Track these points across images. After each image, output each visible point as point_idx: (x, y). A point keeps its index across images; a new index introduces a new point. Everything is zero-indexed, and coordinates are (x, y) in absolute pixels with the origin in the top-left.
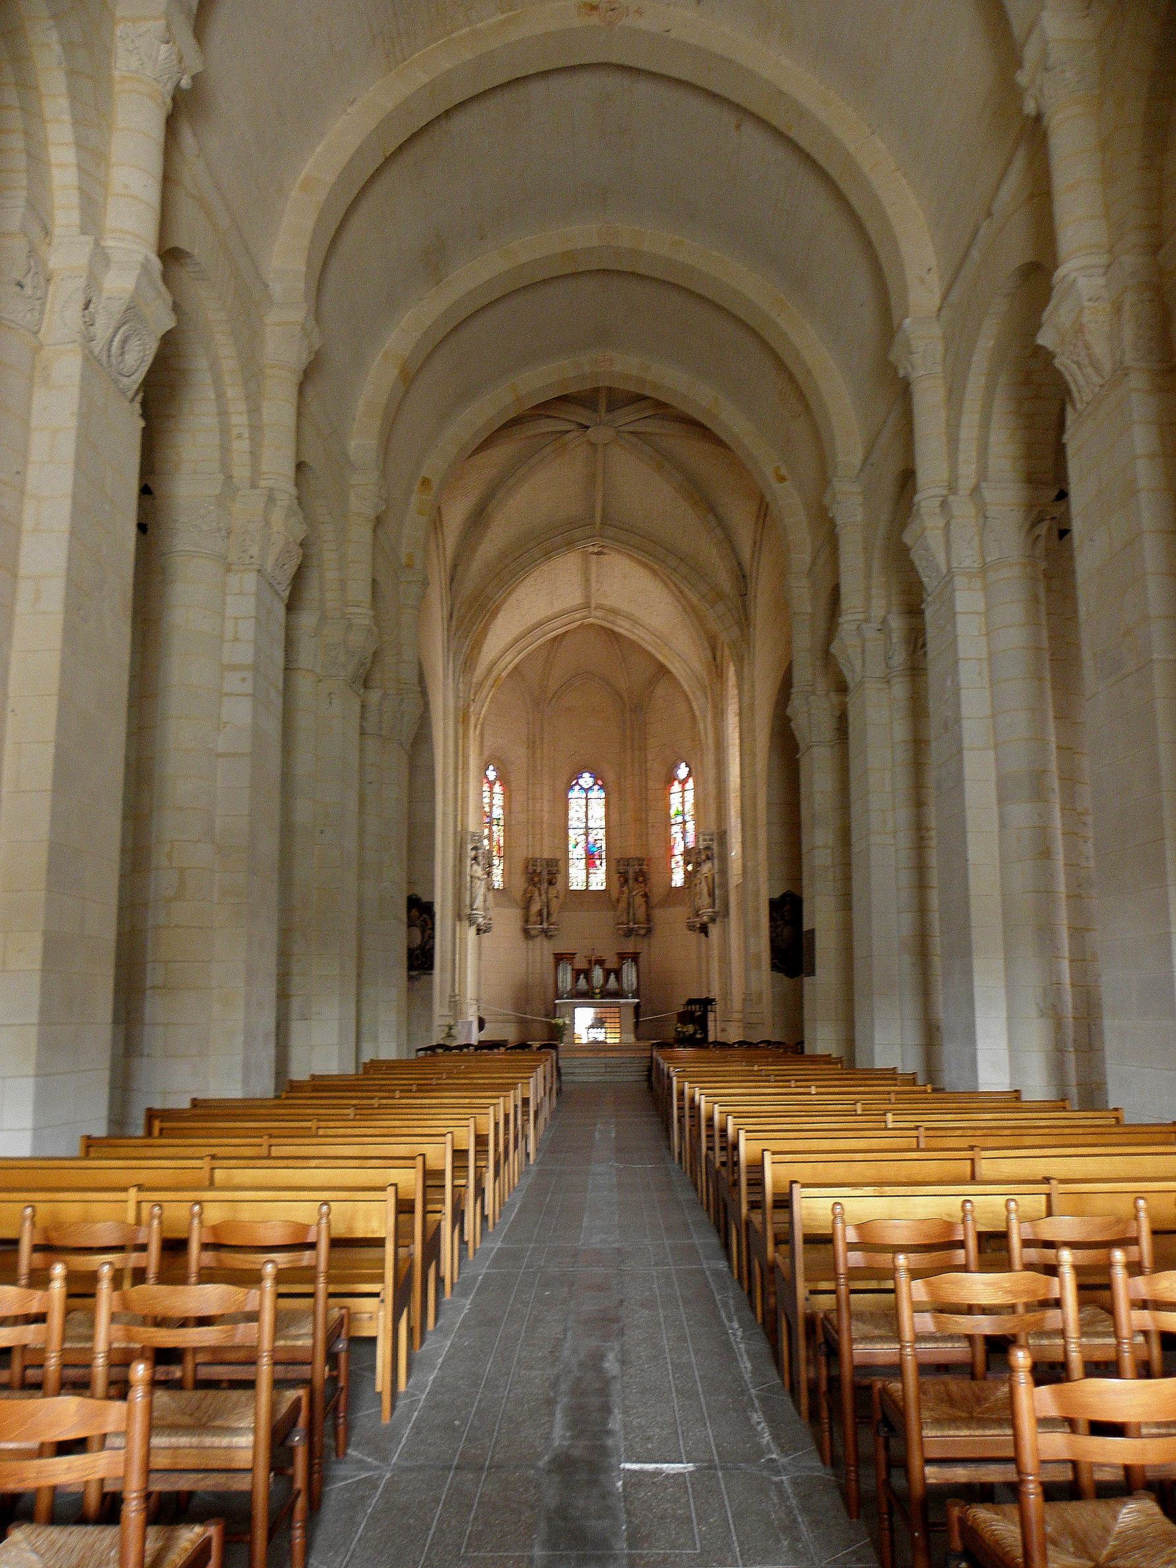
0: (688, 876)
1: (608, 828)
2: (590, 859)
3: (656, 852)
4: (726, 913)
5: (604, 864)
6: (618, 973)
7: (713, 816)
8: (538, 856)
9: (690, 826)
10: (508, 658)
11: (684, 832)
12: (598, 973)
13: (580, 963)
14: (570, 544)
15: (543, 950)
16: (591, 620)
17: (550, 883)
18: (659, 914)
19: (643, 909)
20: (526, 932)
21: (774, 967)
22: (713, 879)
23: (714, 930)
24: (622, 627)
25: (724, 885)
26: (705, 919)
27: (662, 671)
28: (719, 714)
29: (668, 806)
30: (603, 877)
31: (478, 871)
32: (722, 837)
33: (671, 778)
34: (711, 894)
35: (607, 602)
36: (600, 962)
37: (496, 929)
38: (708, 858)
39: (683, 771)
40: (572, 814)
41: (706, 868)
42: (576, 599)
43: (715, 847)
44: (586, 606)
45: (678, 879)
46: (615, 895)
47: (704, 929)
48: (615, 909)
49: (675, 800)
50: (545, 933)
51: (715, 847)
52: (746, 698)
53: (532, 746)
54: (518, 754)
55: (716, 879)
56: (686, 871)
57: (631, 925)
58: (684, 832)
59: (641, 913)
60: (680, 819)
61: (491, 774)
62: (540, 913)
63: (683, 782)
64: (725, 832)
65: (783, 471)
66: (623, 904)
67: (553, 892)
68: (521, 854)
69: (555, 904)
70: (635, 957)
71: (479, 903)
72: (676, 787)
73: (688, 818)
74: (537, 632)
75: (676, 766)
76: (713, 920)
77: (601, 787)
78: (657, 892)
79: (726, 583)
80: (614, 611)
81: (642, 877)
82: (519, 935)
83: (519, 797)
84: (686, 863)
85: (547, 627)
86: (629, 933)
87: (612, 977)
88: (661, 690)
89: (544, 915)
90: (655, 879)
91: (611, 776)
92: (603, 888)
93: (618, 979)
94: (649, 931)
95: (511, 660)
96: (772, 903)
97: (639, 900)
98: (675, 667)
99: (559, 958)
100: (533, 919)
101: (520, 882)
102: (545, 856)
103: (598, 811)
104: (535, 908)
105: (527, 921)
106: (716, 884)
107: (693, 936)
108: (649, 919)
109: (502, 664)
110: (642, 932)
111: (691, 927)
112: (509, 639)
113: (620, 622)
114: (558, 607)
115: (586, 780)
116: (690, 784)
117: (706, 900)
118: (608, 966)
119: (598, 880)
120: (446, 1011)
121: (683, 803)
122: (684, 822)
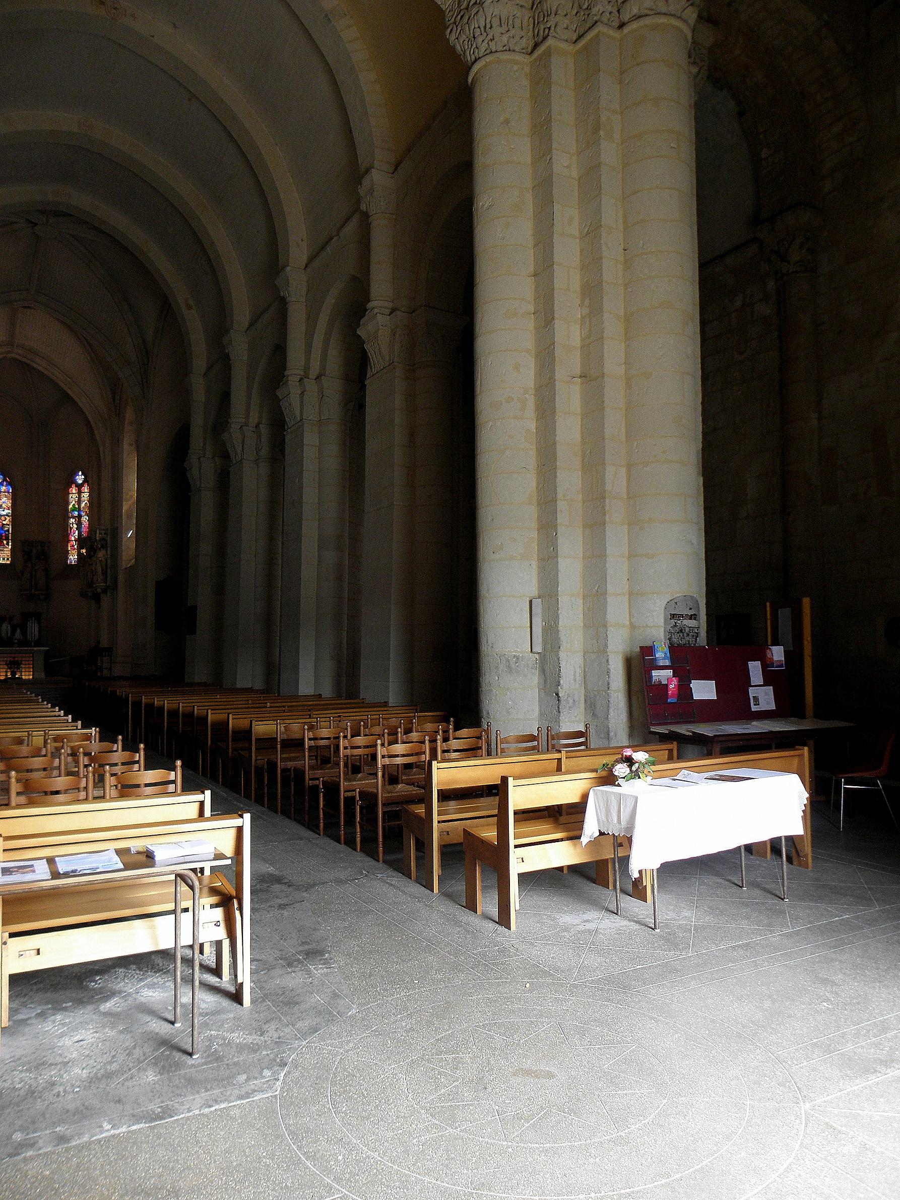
5: (10, 544)
9: (85, 519)
11: (79, 524)
16: (13, 355)
22: (107, 562)
23: (106, 600)
24: (40, 364)
25: (115, 566)
26: (99, 590)
27: (66, 398)
28: (117, 442)
29: (68, 503)
30: (9, 553)
33: (71, 482)
34: (104, 573)
38: (103, 547)
39: (80, 479)
41: (101, 554)
43: (109, 539)
45: (73, 558)
47: (97, 598)
51: (109, 539)
55: (109, 561)
56: (79, 554)
57: (33, 592)
58: (79, 524)
60: (76, 513)
63: (79, 487)
64: (117, 529)
65: (191, 302)
70: (38, 616)
72: (74, 490)
73: (83, 514)
76: (105, 591)
77: (9, 484)
84: (80, 547)
87: (18, 630)
92: (8, 562)
93: (24, 632)
96: (158, 584)
106: (108, 566)
110: (42, 597)
111: (84, 595)
117: (100, 577)
121: (79, 502)
122: (80, 516)
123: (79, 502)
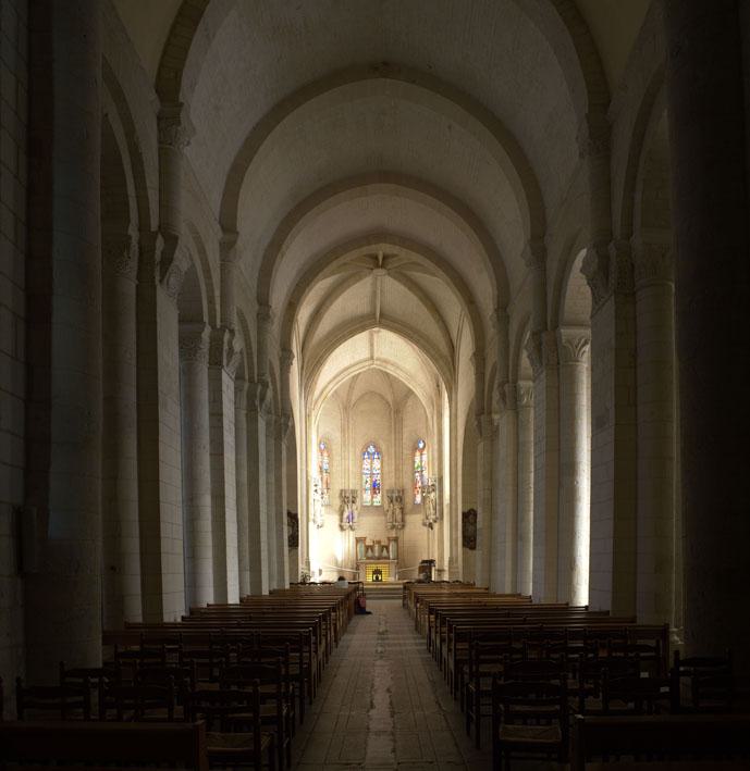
0: (424, 499)
1: (382, 474)
2: (375, 488)
3: (408, 486)
4: (442, 518)
6: (387, 548)
7: (436, 469)
8: (347, 488)
10: (331, 386)
12: (376, 548)
13: (369, 543)
14: (363, 329)
15: (351, 536)
17: (353, 502)
18: (409, 518)
19: (400, 516)
20: (342, 528)
21: (464, 545)
23: (436, 526)
24: (390, 370)
25: (441, 504)
27: (410, 392)
29: (414, 462)
31: (318, 497)
32: (441, 480)
33: (415, 448)
34: (435, 509)
35: (384, 356)
36: (379, 542)
37: (325, 524)
39: (421, 445)
40: (364, 466)
42: (366, 355)
44: (372, 358)
45: (418, 499)
46: (386, 507)
47: (431, 526)
48: (386, 515)
49: (417, 459)
50: (351, 527)
52: (453, 411)
53: (343, 431)
54: (337, 436)
58: (422, 476)
59: (399, 517)
61: (322, 446)
62: (348, 517)
66: (390, 513)
67: (354, 507)
68: (337, 487)
69: (356, 513)
71: (318, 514)
72: (418, 453)
74: (346, 373)
75: (418, 442)
78: (409, 507)
79: (444, 349)
80: (386, 361)
81: (400, 499)
82: (338, 528)
83: (337, 458)
85: (350, 370)
86: (393, 527)
88: (410, 403)
89: (351, 518)
90: (408, 500)
91: (383, 448)
93: (388, 552)
94: (403, 526)
95: (333, 388)
96: (464, 514)
97: (398, 511)
98: (418, 392)
99: (358, 540)
100: (345, 520)
101: (337, 502)
102: (351, 487)
103: (377, 464)
104: (346, 515)
105: (341, 521)
107: (425, 529)
108: (403, 520)
109: (327, 390)
111: (424, 524)
112: (333, 375)
113: (389, 366)
114: (357, 358)
115: (371, 449)
116: (425, 452)
117: (432, 511)
118: (383, 544)
119: (378, 499)
120: (304, 566)
121: (421, 461)
123: (421, 461)
